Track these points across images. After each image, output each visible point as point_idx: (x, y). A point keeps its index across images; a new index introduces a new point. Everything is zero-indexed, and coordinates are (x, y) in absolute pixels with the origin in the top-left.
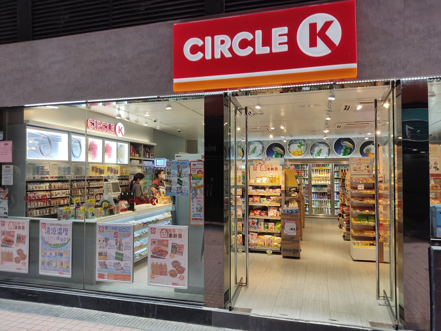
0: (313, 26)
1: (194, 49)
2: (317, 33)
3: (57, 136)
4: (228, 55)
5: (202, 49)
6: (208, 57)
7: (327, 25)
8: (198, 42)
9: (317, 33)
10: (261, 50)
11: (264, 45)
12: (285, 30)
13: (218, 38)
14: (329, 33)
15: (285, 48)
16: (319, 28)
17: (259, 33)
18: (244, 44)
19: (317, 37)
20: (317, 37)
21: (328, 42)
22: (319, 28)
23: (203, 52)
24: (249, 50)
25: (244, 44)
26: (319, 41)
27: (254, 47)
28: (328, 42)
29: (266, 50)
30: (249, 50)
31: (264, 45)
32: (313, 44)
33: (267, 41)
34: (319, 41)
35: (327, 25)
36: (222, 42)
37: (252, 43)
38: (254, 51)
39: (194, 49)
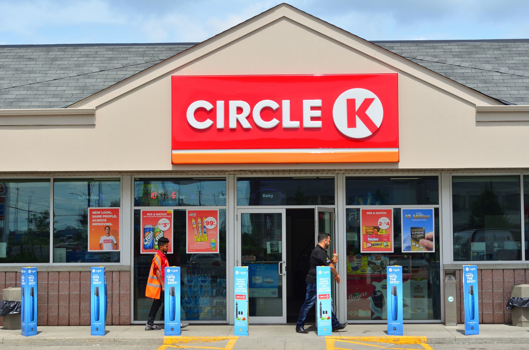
0: (351, 103)
1: (201, 114)
2: (356, 110)
3: (2, 205)
4: (246, 124)
5: (212, 114)
6: (220, 124)
7: (367, 102)
9: (356, 110)
10: (288, 123)
11: (292, 119)
12: (318, 103)
13: (233, 104)
14: (369, 112)
15: (318, 124)
16: (358, 106)
17: (286, 104)
18: (266, 113)
19: (357, 117)
20: (357, 117)
22: (358, 106)
23: (214, 119)
24: (274, 122)
25: (266, 113)
26: (358, 120)
27: (280, 118)
30: (274, 122)
31: (292, 119)
32: (352, 124)
33: (297, 114)
34: (358, 120)
35: (367, 102)
36: (240, 110)
37: (277, 113)
38: (280, 124)
39: (201, 114)
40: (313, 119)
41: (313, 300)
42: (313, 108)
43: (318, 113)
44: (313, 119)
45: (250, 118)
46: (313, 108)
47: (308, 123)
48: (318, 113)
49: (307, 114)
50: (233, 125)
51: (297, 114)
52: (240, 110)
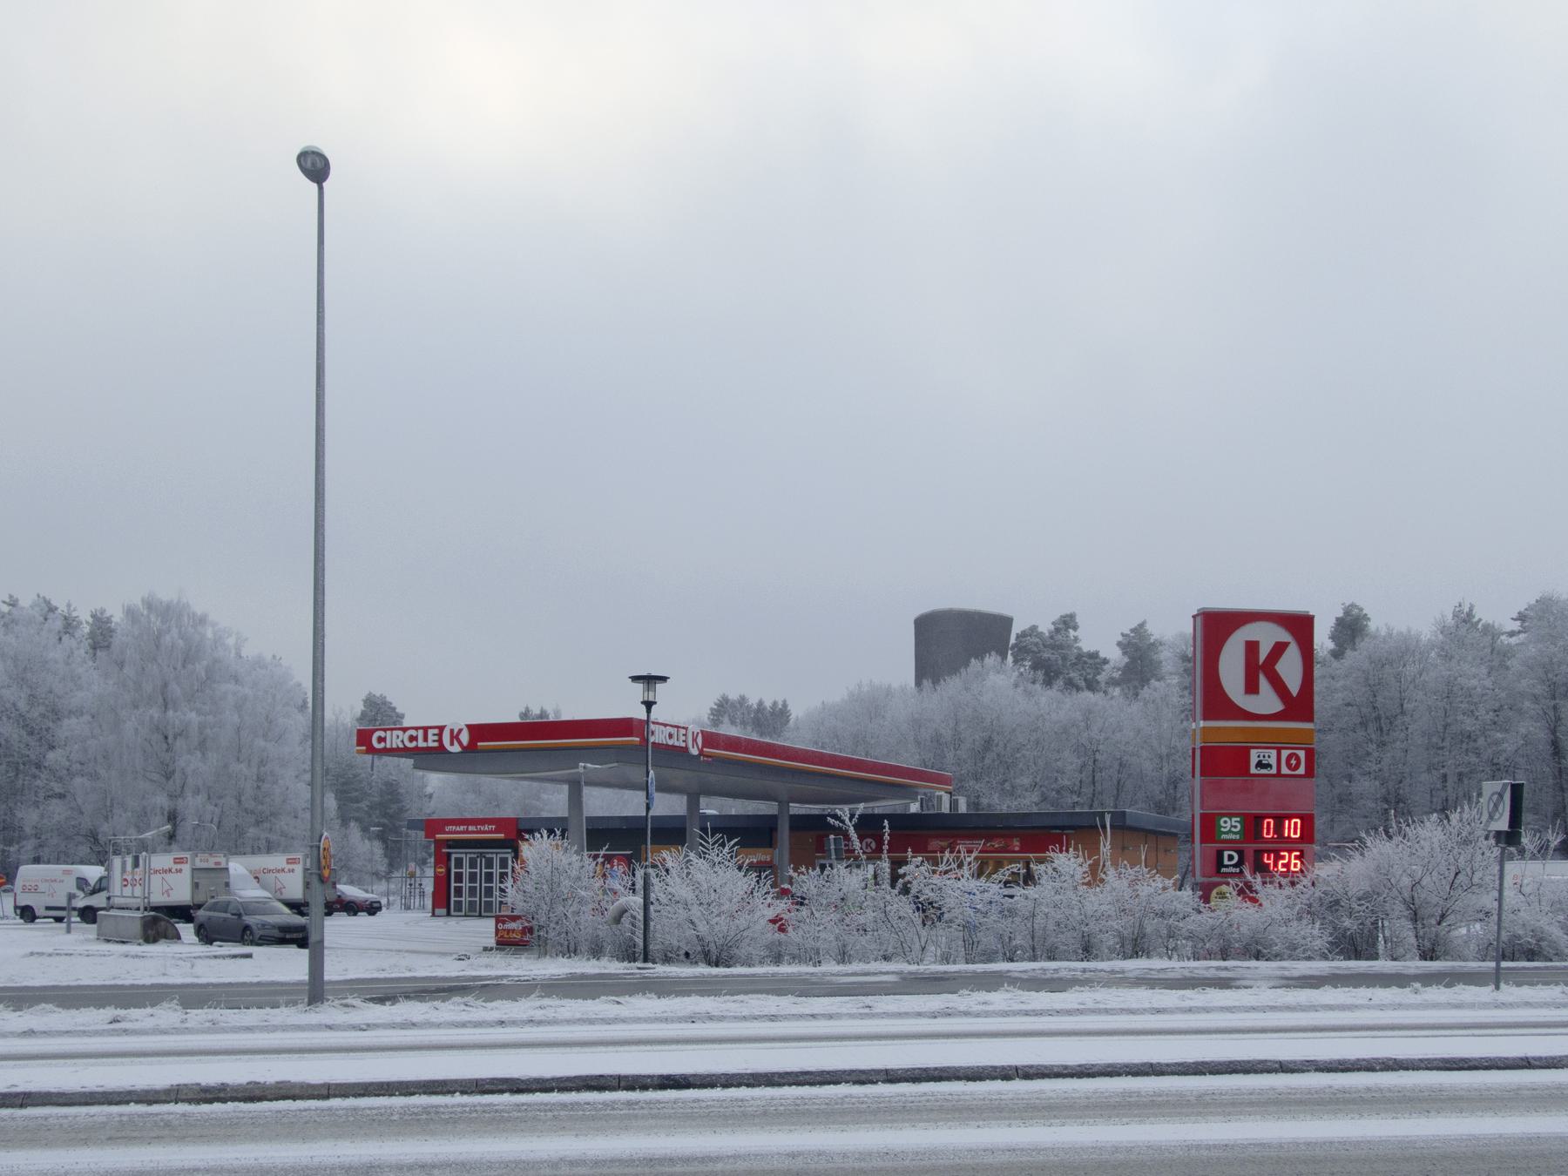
0: (452, 731)
4: (401, 746)
6: (388, 746)
7: (460, 731)
8: (382, 734)
10: (421, 744)
14: (461, 737)
15: (436, 744)
21: (460, 743)
23: (385, 742)
25: (412, 739)
26: (455, 742)
28: (460, 743)
29: (424, 745)
30: (413, 744)
32: (452, 744)
33: (426, 739)
34: (455, 742)
35: (460, 731)
36: (398, 737)
39: (381, 740)
40: (434, 741)
41: (378, 826)
42: (434, 735)
43: (436, 738)
44: (434, 741)
45: (402, 741)
46: (434, 735)
47: (431, 744)
48: (436, 738)
49: (430, 737)
50: (394, 746)
51: (426, 739)
52: (398, 737)
